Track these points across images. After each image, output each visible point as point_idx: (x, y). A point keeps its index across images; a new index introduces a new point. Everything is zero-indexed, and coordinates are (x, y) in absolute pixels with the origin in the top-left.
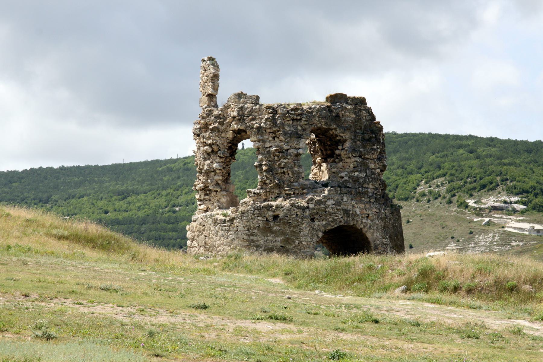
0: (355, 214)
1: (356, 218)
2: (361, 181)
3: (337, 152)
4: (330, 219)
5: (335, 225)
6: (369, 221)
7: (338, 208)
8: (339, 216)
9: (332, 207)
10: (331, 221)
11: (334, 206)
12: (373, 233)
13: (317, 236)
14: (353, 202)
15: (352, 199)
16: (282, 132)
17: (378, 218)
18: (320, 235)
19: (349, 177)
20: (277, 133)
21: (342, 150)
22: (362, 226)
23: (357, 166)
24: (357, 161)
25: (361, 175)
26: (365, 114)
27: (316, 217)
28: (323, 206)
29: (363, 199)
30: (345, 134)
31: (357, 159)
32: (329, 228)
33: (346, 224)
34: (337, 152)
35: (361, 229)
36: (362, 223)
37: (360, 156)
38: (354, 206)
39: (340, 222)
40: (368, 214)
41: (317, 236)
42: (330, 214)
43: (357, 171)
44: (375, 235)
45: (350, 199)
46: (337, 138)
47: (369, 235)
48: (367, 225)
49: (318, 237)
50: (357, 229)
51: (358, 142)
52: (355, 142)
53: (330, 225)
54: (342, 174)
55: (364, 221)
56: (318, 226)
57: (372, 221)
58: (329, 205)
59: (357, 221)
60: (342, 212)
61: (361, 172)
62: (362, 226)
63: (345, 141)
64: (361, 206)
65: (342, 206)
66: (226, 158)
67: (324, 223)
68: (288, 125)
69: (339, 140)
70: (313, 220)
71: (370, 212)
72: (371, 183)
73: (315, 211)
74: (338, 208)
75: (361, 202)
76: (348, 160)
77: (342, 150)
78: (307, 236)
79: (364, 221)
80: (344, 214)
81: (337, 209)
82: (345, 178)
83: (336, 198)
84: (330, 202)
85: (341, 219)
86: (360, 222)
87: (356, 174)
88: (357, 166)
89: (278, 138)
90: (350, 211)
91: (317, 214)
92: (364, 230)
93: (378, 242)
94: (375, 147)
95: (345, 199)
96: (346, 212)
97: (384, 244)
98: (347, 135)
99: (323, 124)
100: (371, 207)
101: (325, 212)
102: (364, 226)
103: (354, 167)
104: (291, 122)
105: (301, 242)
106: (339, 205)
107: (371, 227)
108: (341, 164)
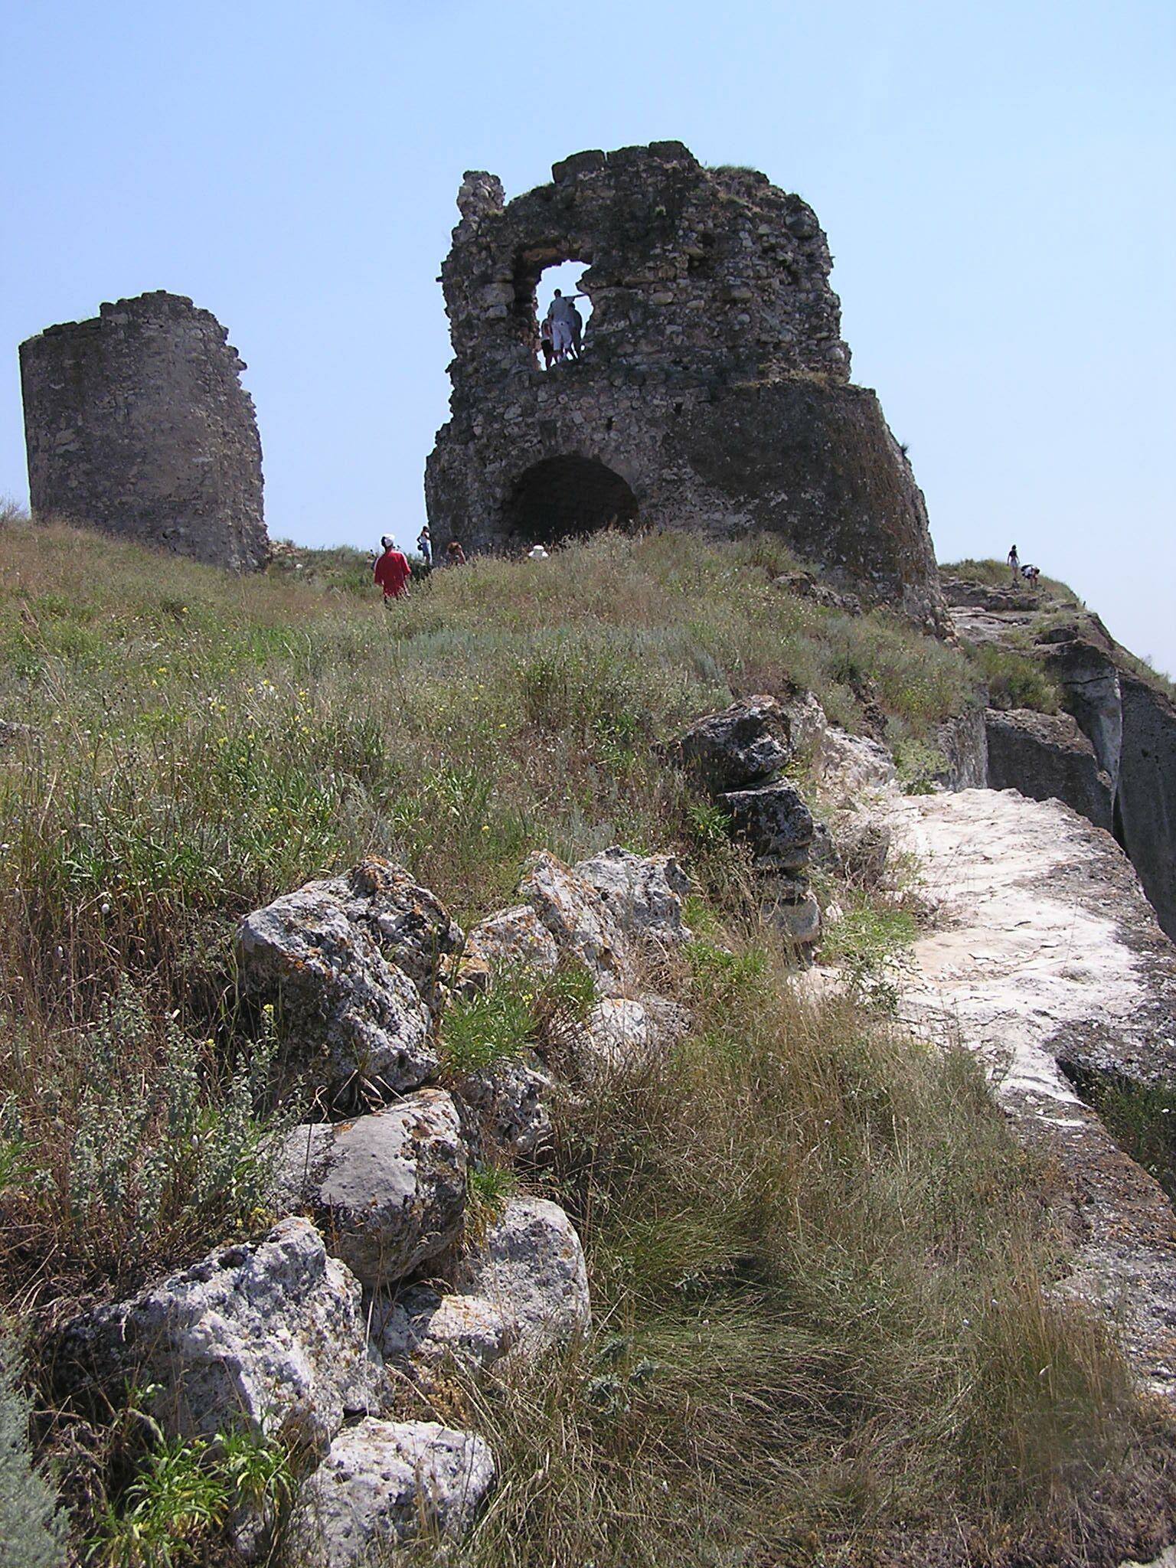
0: (570, 426)
7: (530, 420)
10: (518, 457)
12: (628, 461)
14: (563, 399)
15: (559, 392)
17: (638, 421)
22: (596, 451)
24: (605, 297)
25: (612, 328)
26: (650, 181)
28: (496, 426)
31: (604, 293)
32: (515, 471)
35: (597, 457)
37: (618, 284)
38: (565, 409)
39: (539, 451)
40: (610, 419)
44: (635, 463)
47: (620, 469)
49: (495, 500)
50: (561, 458)
51: (614, 252)
53: (516, 465)
55: (597, 437)
56: (493, 473)
57: (620, 432)
59: (579, 442)
62: (596, 451)
64: (587, 401)
71: (611, 413)
72: (643, 341)
74: (530, 420)
79: (597, 437)
81: (527, 425)
83: (522, 399)
86: (588, 443)
90: (555, 421)
92: (604, 458)
93: (648, 481)
94: (658, 251)
95: (542, 395)
96: (547, 428)
97: (668, 482)
101: (505, 437)
102: (601, 450)
106: (532, 415)
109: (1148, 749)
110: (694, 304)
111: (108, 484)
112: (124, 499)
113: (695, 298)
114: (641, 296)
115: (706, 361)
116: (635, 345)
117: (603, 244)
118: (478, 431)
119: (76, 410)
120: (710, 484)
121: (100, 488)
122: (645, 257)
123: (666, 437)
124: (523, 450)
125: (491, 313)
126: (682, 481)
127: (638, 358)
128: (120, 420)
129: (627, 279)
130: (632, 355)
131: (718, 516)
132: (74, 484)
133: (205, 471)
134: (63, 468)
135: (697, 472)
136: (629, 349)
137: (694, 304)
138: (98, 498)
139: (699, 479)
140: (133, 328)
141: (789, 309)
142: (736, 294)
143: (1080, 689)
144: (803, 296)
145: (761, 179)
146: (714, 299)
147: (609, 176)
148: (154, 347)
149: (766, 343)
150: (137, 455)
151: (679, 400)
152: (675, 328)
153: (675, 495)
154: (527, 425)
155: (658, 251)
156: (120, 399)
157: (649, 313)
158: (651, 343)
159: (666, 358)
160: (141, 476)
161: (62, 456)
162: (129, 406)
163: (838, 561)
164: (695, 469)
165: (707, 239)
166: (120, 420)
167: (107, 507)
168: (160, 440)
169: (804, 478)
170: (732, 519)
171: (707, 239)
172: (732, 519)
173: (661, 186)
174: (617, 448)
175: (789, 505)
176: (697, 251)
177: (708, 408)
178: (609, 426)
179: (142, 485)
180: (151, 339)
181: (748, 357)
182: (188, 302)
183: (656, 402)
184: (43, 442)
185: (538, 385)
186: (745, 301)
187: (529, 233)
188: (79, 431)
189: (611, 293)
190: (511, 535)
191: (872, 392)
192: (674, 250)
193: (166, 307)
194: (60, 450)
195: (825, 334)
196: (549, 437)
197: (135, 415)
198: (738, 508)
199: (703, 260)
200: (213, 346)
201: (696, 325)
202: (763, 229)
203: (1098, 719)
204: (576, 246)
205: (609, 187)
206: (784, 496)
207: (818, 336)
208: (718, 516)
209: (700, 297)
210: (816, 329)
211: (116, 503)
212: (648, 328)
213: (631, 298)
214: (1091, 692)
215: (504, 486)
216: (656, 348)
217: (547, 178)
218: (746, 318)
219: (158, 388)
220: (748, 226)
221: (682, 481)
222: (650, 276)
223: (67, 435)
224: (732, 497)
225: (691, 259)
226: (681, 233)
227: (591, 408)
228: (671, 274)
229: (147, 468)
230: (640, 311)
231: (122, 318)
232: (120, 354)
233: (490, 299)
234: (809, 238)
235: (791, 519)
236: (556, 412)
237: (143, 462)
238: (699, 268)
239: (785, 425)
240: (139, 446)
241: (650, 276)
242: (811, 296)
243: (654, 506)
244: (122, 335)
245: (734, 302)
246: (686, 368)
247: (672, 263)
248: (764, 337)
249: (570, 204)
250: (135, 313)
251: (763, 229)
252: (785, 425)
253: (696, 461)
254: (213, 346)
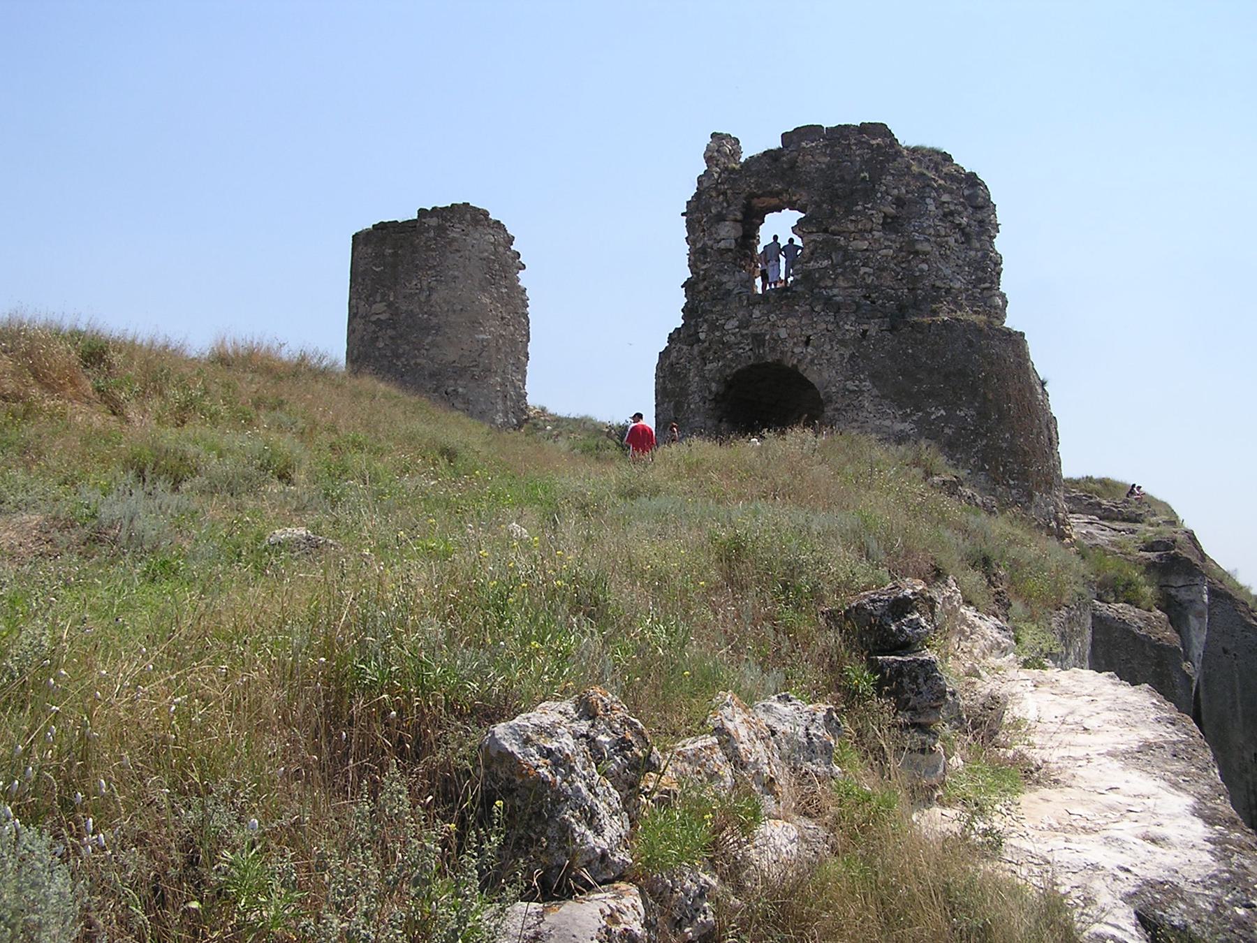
1: (780, 347)
7: (745, 332)
10: (732, 360)
14: (773, 317)
15: (770, 312)
17: (831, 341)
25: (817, 265)
31: (813, 237)
32: (728, 371)
35: (795, 367)
37: (826, 231)
38: (774, 325)
40: (808, 338)
44: (825, 375)
47: (812, 377)
48: (805, 357)
49: (710, 392)
50: (767, 365)
53: (730, 367)
55: (797, 350)
59: (782, 352)
64: (791, 321)
74: (745, 332)
79: (797, 350)
81: (742, 336)
90: (765, 335)
92: (801, 369)
93: (834, 389)
94: (859, 208)
95: (756, 313)
96: (758, 339)
97: (851, 392)
101: (723, 343)
102: (799, 361)
106: (747, 327)
109: (1228, 647)
110: (884, 252)
111: (407, 348)
112: (419, 361)
113: (886, 247)
114: (842, 242)
115: (890, 298)
116: (834, 280)
117: (816, 198)
118: (702, 336)
119: (390, 289)
120: (884, 397)
121: (401, 351)
122: (849, 211)
123: (852, 356)
124: (737, 355)
125: (722, 245)
126: (862, 392)
127: (836, 291)
128: (423, 299)
129: (833, 227)
130: (831, 288)
131: (888, 423)
132: (381, 345)
133: (484, 346)
134: (374, 332)
135: (874, 385)
136: (829, 283)
137: (884, 252)
138: (398, 357)
139: (875, 392)
140: (441, 230)
141: (960, 262)
142: (919, 247)
143: (1173, 592)
144: (972, 253)
145: (947, 158)
146: (901, 249)
147: (826, 146)
148: (455, 246)
149: (940, 288)
150: (432, 328)
151: (866, 327)
152: (867, 270)
153: (855, 403)
154: (742, 336)
155: (859, 208)
156: (425, 283)
157: (847, 255)
158: (846, 279)
159: (858, 293)
160: (434, 344)
161: (374, 323)
162: (431, 289)
163: (983, 469)
164: (873, 383)
165: (899, 202)
166: (423, 299)
167: (404, 366)
168: (452, 318)
169: (960, 399)
170: (899, 426)
171: (899, 202)
172: (899, 426)
173: (866, 157)
174: (812, 361)
175: (946, 419)
176: (891, 210)
177: (888, 335)
178: (807, 343)
179: (433, 351)
180: (454, 239)
181: (924, 298)
182: (486, 214)
183: (847, 327)
184: (361, 311)
185: (754, 305)
186: (926, 253)
187: (758, 185)
188: (390, 305)
189: (820, 237)
190: (720, 421)
191: (1022, 334)
192: (872, 208)
193: (468, 216)
194: (374, 318)
195: (987, 285)
196: (759, 347)
197: (435, 296)
198: (904, 419)
199: (894, 218)
200: (501, 249)
201: (884, 269)
202: (946, 198)
203: (1187, 619)
204: (794, 198)
205: (825, 154)
206: (942, 412)
207: (983, 286)
208: (888, 423)
209: (890, 247)
210: (981, 280)
211: (412, 362)
212: (845, 268)
213: (835, 243)
214: (1183, 595)
215: (718, 382)
216: (851, 284)
217: (777, 144)
218: (925, 267)
219: (456, 277)
220: (934, 194)
221: (862, 392)
222: (851, 227)
223: (380, 307)
224: (901, 408)
225: (886, 216)
226: (879, 195)
227: (795, 327)
228: (868, 227)
229: (439, 338)
230: (841, 253)
231: (433, 222)
232: (429, 249)
233: (723, 234)
234: (982, 207)
235: (946, 430)
236: (766, 327)
237: (437, 334)
238: (891, 224)
239: (949, 356)
240: (435, 321)
241: (851, 227)
242: (979, 254)
243: (837, 409)
244: (432, 234)
245: (917, 253)
246: (873, 302)
247: (870, 218)
248: (938, 283)
249: (793, 165)
250: (444, 219)
251: (946, 198)
252: (949, 356)
253: (874, 377)
254: (501, 249)
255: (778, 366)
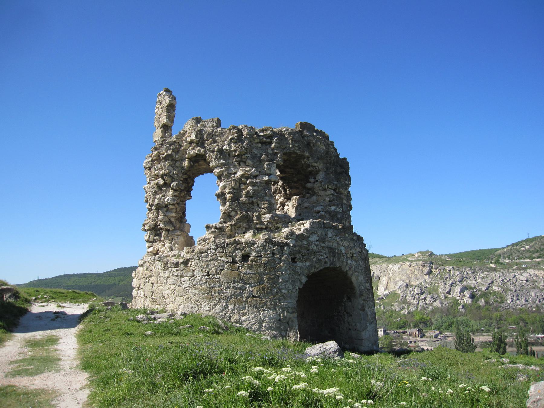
0: (340, 254)
2: (339, 216)
3: (309, 185)
4: (314, 260)
5: (320, 267)
6: (354, 263)
7: (323, 245)
8: (324, 256)
9: (315, 244)
10: (316, 262)
11: (318, 243)
13: (300, 281)
14: (338, 239)
15: (336, 236)
16: (249, 155)
18: (304, 279)
19: (325, 212)
20: (243, 157)
21: (314, 183)
22: (347, 269)
23: (333, 200)
27: (298, 256)
28: (305, 243)
29: (347, 235)
30: (318, 164)
32: (313, 270)
33: (332, 266)
34: (309, 185)
35: (347, 271)
36: (347, 264)
37: (335, 190)
38: (338, 243)
39: (326, 262)
41: (300, 281)
42: (314, 253)
43: (334, 205)
44: (360, 278)
45: (335, 234)
46: (309, 169)
47: (354, 279)
48: (352, 267)
49: (301, 283)
51: (331, 175)
52: (329, 174)
54: (318, 208)
55: (349, 262)
56: (301, 268)
57: (356, 262)
58: (312, 242)
59: (343, 262)
60: (327, 250)
61: (338, 206)
62: (347, 269)
63: (317, 172)
64: (346, 243)
65: (327, 243)
66: (181, 191)
67: (308, 264)
68: (257, 148)
69: (311, 172)
70: (294, 260)
71: (354, 252)
73: (297, 248)
74: (323, 245)
75: (345, 239)
76: (323, 193)
77: (314, 183)
78: (287, 281)
80: (330, 252)
81: (322, 247)
82: (321, 212)
84: (314, 238)
85: (327, 260)
86: (345, 264)
87: (333, 208)
88: (333, 200)
89: (245, 162)
90: (336, 249)
91: (299, 252)
92: (350, 273)
95: (330, 235)
96: (331, 250)
98: (320, 165)
99: (297, 148)
100: (355, 246)
102: (350, 269)
103: (330, 201)
104: (260, 145)
105: (280, 290)
106: (324, 242)
107: (356, 270)
108: (314, 198)
255: (335, 269)
